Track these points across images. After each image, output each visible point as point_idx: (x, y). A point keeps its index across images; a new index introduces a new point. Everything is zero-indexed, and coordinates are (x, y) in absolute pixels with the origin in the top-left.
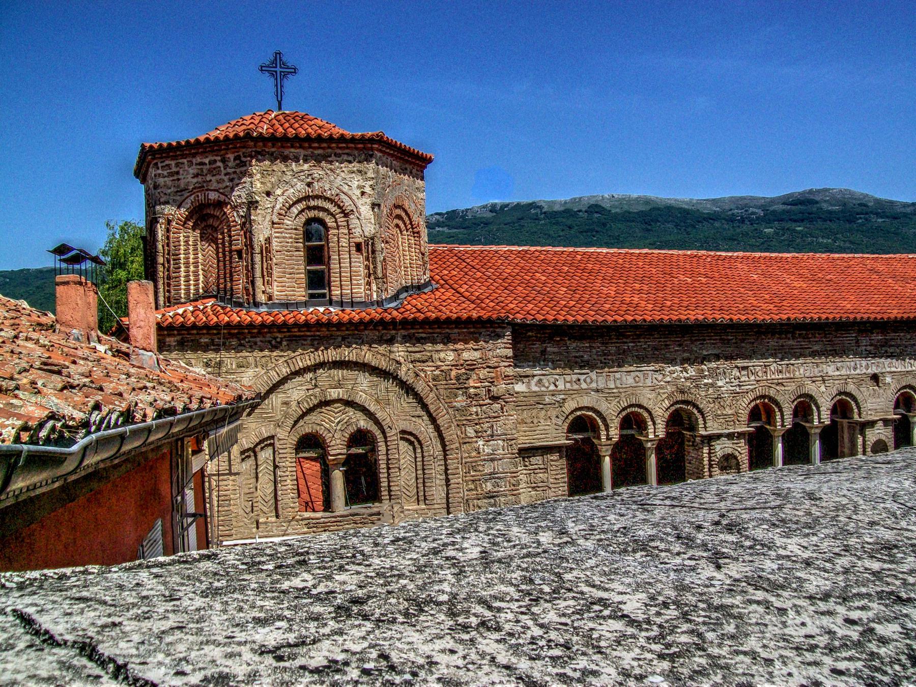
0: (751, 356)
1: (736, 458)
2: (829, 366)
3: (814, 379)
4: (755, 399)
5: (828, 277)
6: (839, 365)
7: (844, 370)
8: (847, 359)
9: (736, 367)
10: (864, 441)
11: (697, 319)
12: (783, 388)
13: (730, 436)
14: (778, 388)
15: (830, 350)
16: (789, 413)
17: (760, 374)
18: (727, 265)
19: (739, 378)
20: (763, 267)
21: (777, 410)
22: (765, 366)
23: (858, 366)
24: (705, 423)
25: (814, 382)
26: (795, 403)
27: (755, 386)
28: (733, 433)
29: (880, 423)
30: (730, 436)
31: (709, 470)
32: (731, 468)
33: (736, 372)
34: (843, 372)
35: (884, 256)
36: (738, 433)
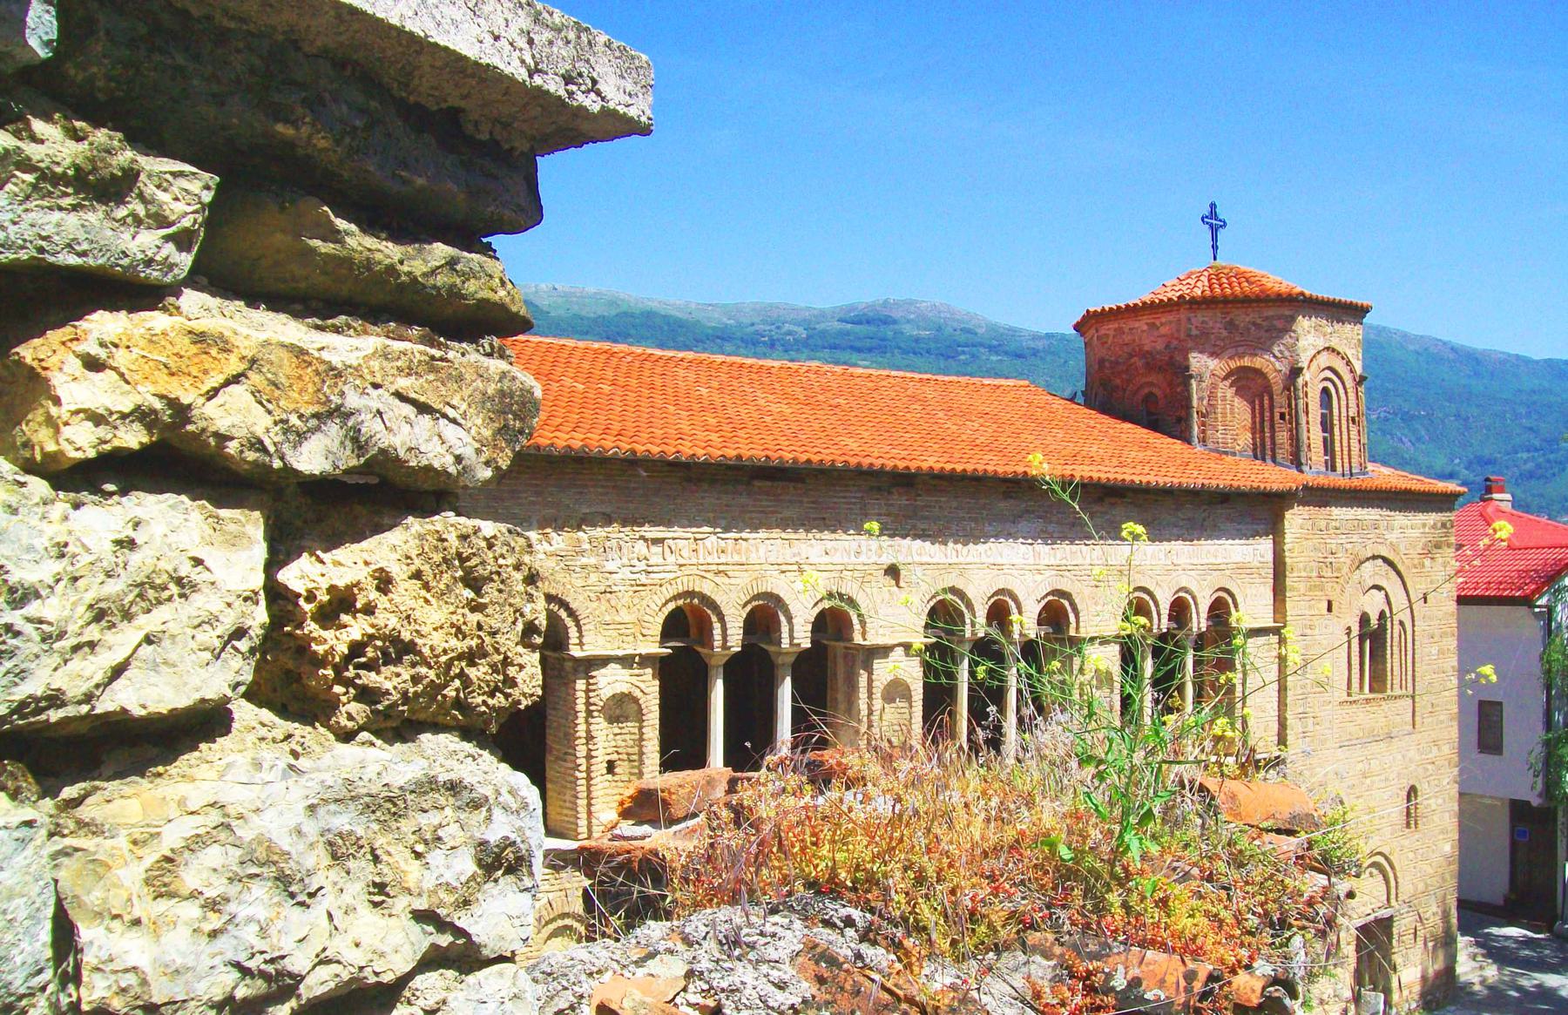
0: (669, 520)
1: (636, 701)
2: (811, 545)
3: (784, 568)
4: (675, 598)
5: (832, 402)
6: (829, 545)
7: (838, 554)
8: (845, 537)
9: (642, 538)
10: (870, 681)
11: (569, 447)
12: (726, 580)
13: (626, 661)
14: (717, 579)
15: (815, 519)
16: (737, 625)
17: (685, 553)
18: (659, 370)
19: (646, 558)
20: (724, 377)
21: (714, 619)
22: (696, 540)
23: (864, 549)
24: (581, 636)
25: (783, 572)
26: (749, 608)
27: (672, 576)
28: (633, 657)
29: (900, 651)
30: (626, 661)
31: (587, 722)
32: (627, 719)
33: (641, 545)
34: (837, 558)
35: (940, 378)
36: (640, 655)
